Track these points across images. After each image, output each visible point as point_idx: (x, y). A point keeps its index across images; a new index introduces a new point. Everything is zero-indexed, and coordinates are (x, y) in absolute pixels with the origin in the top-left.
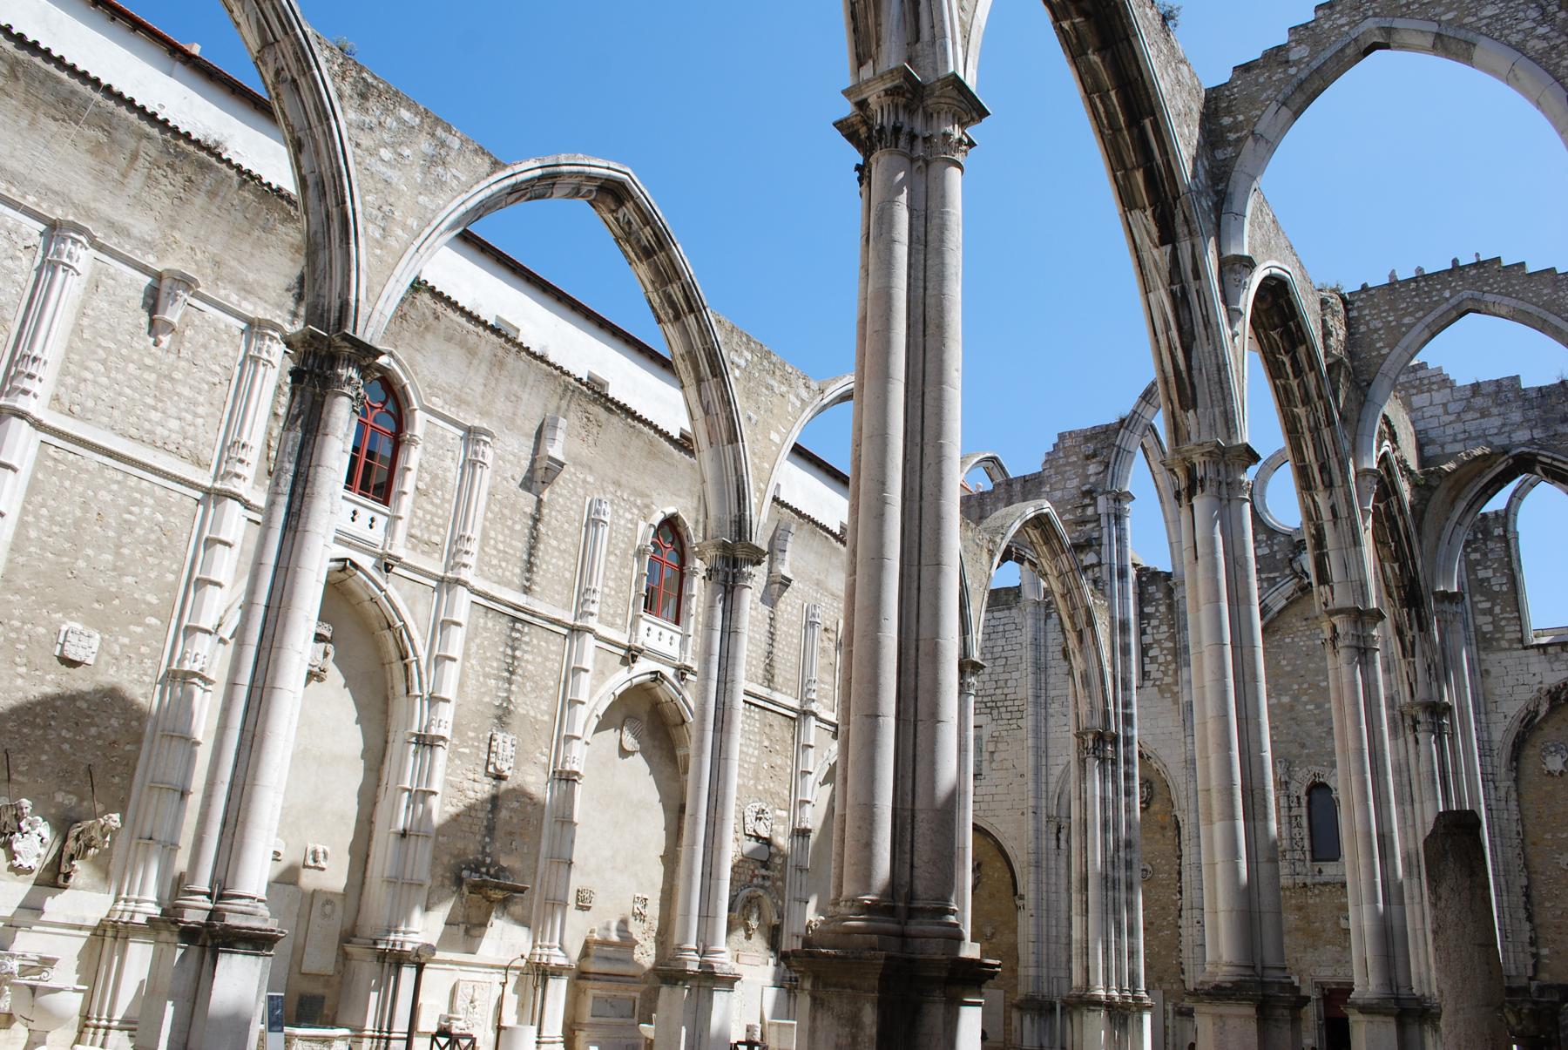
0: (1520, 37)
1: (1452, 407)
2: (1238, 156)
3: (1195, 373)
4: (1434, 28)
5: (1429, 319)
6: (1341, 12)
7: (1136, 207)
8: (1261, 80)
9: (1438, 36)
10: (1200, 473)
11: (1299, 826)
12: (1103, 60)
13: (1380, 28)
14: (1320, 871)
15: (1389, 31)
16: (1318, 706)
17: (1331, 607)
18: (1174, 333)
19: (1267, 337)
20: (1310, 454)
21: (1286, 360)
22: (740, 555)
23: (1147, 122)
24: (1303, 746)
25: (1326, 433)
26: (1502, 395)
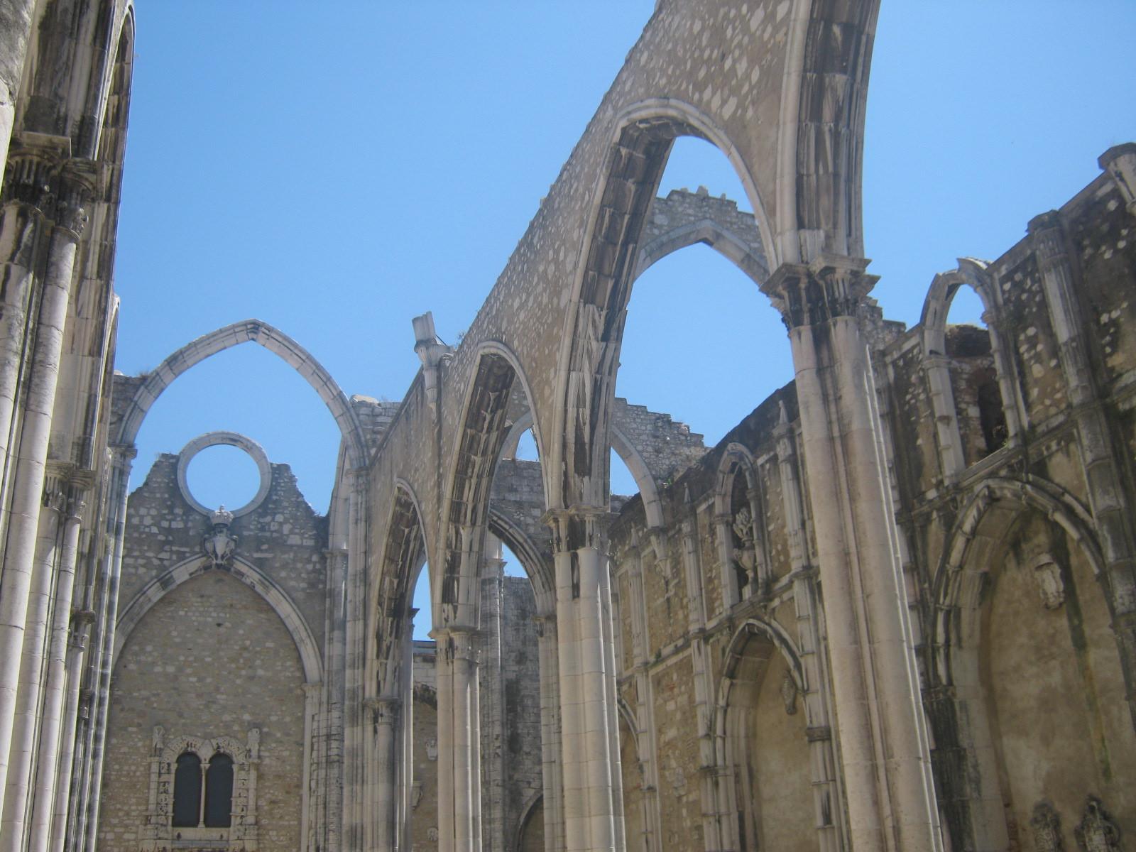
4: (748, 250)
6: (690, 204)
7: (593, 302)
9: (748, 256)
10: (588, 529)
11: (166, 792)
12: (637, 191)
14: (179, 836)
15: (719, 236)
16: (201, 680)
17: (451, 622)
18: (587, 412)
19: (482, 395)
20: (468, 495)
21: (488, 417)
22: (77, 484)
23: (631, 247)
24: (181, 715)
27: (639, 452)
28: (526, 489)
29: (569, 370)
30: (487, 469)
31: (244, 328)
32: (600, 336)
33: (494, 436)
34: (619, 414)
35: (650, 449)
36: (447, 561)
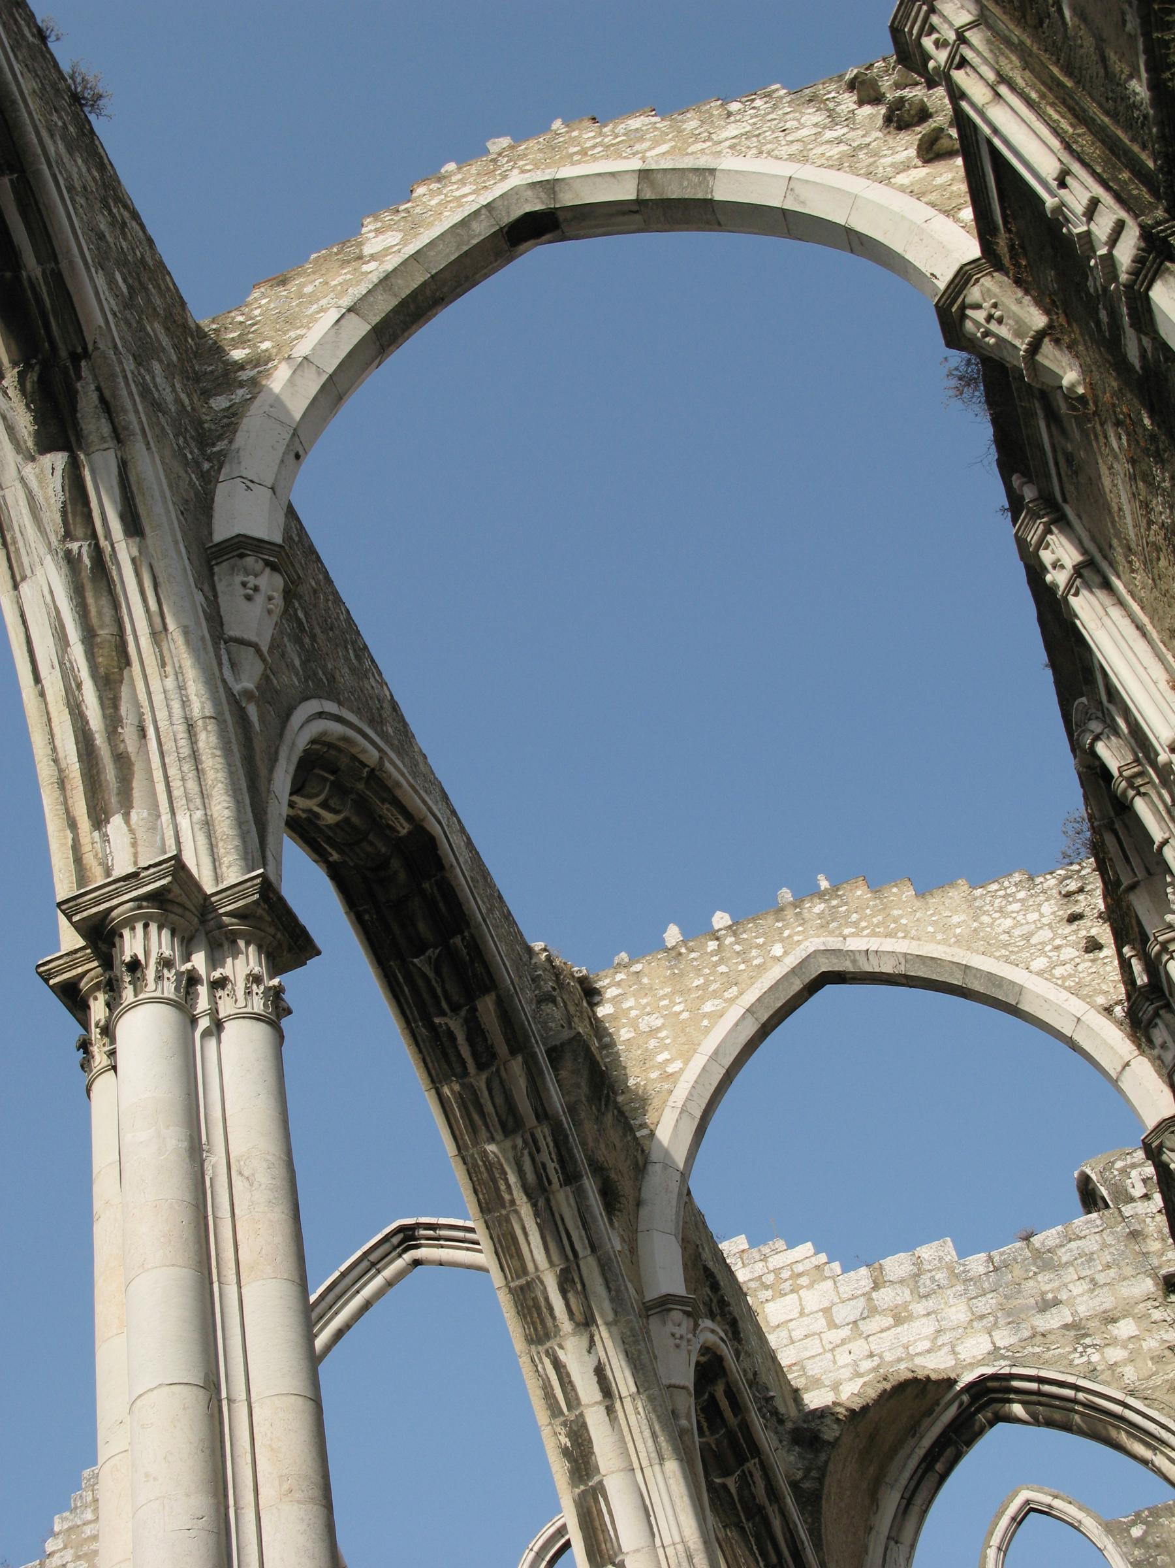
0: (796, 147)
1: (845, 1313)
2: (253, 398)
3: (128, 733)
5: (751, 997)
8: (308, 289)
13: (533, 185)
25: (563, 1199)
26: (925, 1279)
27: (1040, 974)
28: (1079, 1288)
29: (16, 587)
30: (552, 1166)
31: (386, 1247)
32: (30, 444)
33: (517, 1066)
34: (956, 919)
35: (1069, 953)
36: (566, 1452)
